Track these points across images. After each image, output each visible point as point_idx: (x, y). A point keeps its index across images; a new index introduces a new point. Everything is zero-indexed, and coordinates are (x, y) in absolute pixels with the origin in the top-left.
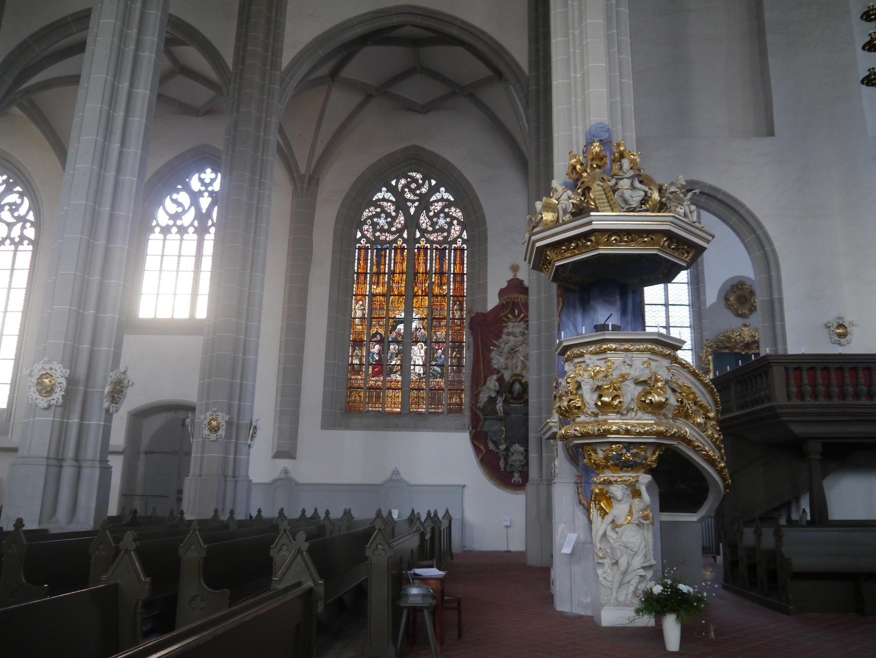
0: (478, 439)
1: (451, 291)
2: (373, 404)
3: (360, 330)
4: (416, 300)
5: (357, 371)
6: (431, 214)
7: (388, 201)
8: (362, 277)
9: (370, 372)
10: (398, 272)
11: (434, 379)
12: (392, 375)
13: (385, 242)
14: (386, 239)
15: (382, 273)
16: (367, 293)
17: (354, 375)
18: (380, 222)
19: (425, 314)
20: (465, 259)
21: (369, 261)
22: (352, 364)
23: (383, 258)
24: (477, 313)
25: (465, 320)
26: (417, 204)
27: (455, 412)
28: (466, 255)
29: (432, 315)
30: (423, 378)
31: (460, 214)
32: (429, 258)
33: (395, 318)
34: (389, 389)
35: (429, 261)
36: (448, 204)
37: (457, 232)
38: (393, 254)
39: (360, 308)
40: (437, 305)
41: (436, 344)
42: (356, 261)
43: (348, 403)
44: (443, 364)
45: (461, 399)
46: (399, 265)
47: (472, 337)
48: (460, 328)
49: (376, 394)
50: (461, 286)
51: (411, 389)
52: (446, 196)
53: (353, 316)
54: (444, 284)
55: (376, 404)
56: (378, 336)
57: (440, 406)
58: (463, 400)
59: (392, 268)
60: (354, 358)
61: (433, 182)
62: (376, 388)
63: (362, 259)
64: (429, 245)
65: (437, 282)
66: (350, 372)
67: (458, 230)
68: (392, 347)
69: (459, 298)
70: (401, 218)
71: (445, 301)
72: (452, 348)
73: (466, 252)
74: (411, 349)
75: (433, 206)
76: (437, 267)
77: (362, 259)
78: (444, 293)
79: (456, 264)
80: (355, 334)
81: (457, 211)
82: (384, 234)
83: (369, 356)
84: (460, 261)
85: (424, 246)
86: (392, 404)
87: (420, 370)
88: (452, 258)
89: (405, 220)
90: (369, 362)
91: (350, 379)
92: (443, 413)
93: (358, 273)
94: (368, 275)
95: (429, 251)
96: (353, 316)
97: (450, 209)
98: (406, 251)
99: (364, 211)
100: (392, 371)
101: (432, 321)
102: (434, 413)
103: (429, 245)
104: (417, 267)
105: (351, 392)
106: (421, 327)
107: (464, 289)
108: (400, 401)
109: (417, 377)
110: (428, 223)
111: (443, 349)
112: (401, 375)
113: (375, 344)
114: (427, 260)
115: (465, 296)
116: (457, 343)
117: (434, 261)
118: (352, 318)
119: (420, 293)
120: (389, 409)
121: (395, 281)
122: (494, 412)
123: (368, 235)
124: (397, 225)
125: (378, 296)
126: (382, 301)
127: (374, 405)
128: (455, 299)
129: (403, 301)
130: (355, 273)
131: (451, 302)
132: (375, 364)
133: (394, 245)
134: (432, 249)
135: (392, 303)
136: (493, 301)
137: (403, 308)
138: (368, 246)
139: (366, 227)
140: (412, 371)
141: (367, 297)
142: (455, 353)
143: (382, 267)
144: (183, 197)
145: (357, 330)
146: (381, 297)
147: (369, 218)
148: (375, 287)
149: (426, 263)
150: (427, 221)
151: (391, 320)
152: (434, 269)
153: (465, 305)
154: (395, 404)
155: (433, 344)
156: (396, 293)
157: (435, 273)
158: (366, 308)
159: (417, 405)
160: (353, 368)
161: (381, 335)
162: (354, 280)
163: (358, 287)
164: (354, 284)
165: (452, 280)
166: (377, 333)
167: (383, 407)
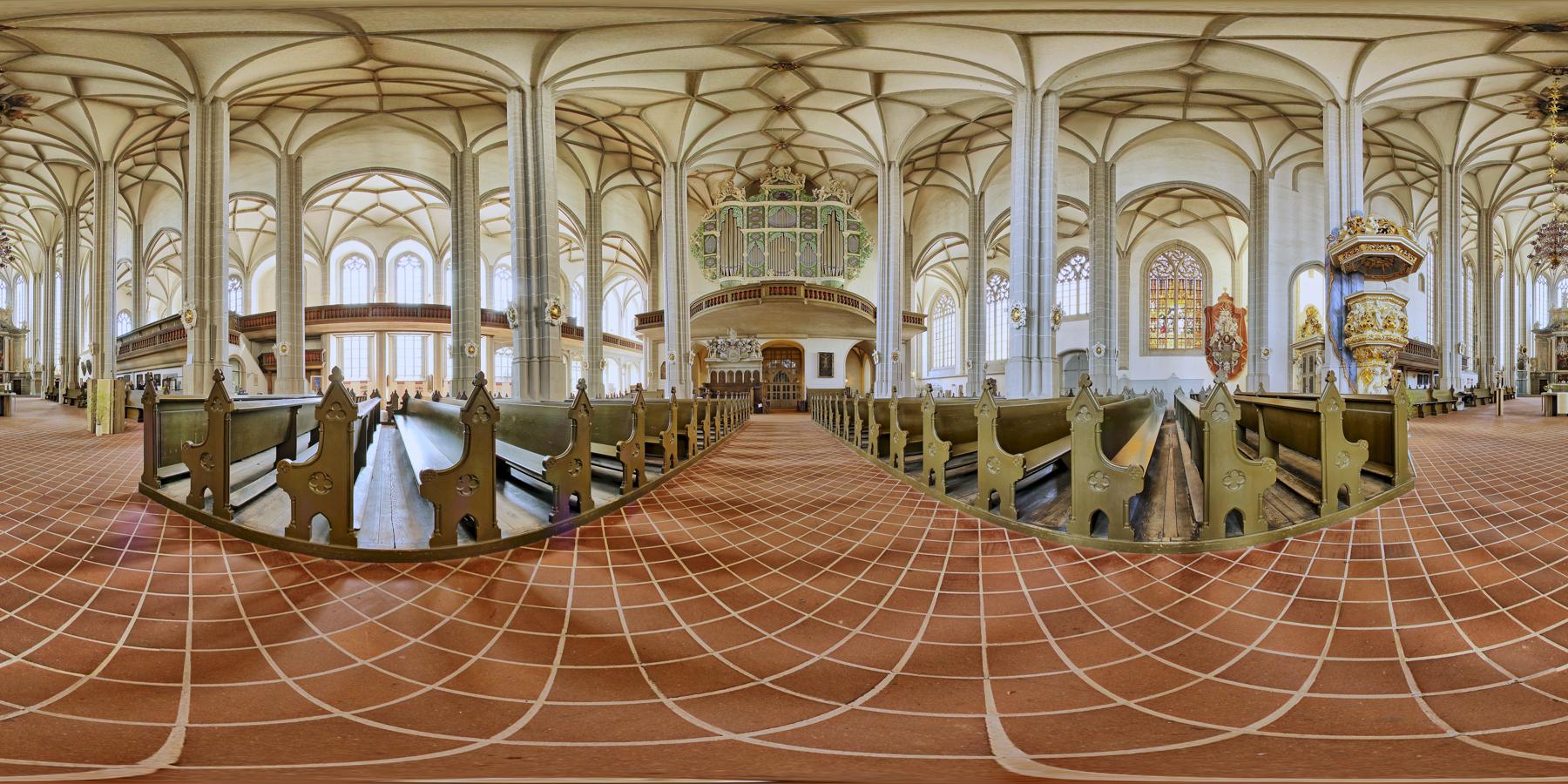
0: (1210, 358)
36: (1193, 262)
70: (1171, 268)
101: (1186, 309)
122: (1217, 348)
136: (1215, 302)
144: (1069, 268)
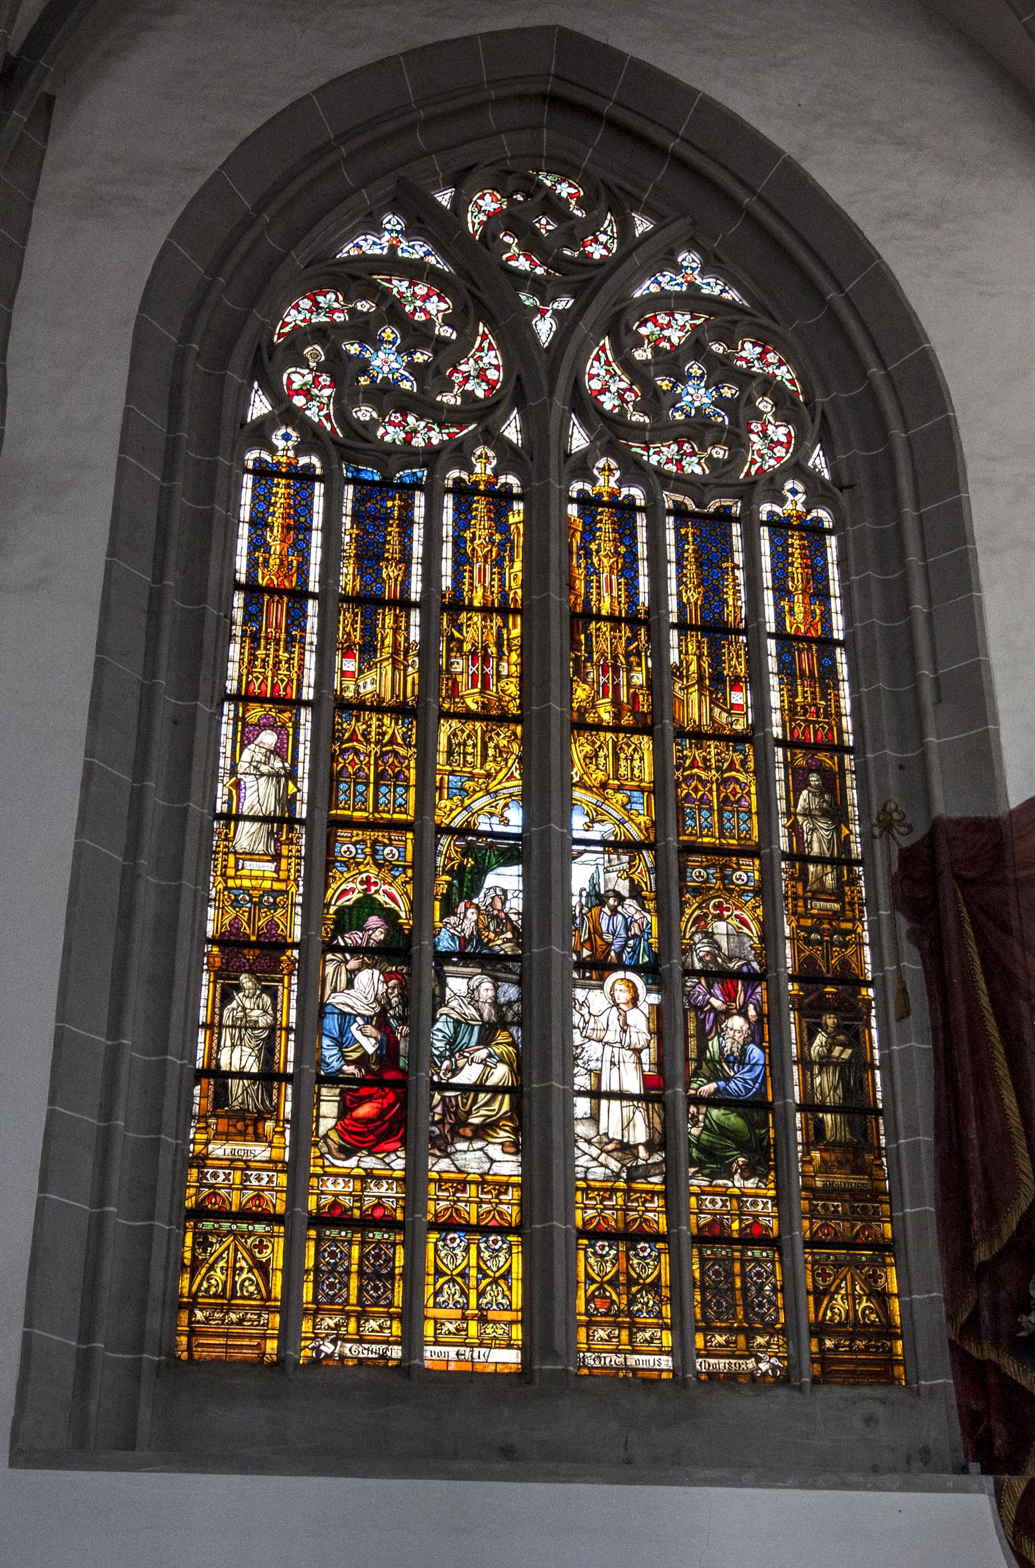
1: (776, 717)
2: (348, 1315)
3: (267, 884)
4: (588, 748)
5: (241, 1114)
6: (643, 354)
7: (415, 271)
8: (277, 612)
9: (326, 1125)
10: (476, 603)
11: (713, 1176)
12: (462, 1146)
13: (407, 454)
14: (407, 441)
15: (393, 603)
16: (308, 694)
17: (227, 1136)
18: (377, 363)
19: (642, 819)
20: (833, 572)
21: (316, 538)
22: (218, 1076)
23: (394, 529)
24: (936, 826)
25: (859, 870)
26: (564, 303)
27: (853, 1378)
28: (832, 554)
29: (681, 830)
30: (646, 1172)
31: (784, 373)
32: (642, 550)
33: (466, 831)
34: (445, 1226)
35: (643, 568)
37: (780, 451)
38: (448, 516)
39: (264, 769)
40: (704, 783)
41: (710, 987)
42: (244, 530)
43: (182, 1306)
44: (762, 1093)
45: (882, 1297)
46: (482, 571)
47: (916, 952)
48: (836, 906)
49: (363, 1257)
50: (824, 696)
51: (582, 1233)
52: (712, 287)
53: (220, 807)
54: (736, 684)
55: (362, 1316)
56: (373, 921)
57: (760, 1340)
58: (895, 1305)
59: (447, 582)
60: (226, 1034)
61: (642, 225)
62: (366, 1223)
63: (277, 521)
64: (637, 493)
65: (693, 667)
66: (203, 1117)
67: (784, 439)
68: (456, 985)
69: (821, 756)
71: (744, 763)
72: (801, 1009)
73: (832, 541)
74: (569, 1004)
75: (650, 325)
76: (693, 596)
77: (277, 521)
78: (739, 727)
79: (790, 594)
80: (236, 903)
81: (771, 357)
82: (396, 417)
83: (321, 1033)
84: (806, 581)
85: (613, 494)
86: (465, 1318)
87: (626, 1125)
88: (766, 562)
89: (508, 367)
90: (321, 1062)
91: (201, 1161)
92: (785, 1379)
93: (252, 589)
94: (312, 607)
95: (641, 520)
96: (220, 807)
97: (731, 344)
98: (518, 506)
99: (289, 300)
100: (466, 1124)
102: (732, 1377)
103: (637, 493)
104: (580, 585)
105: (202, 1241)
106: (623, 888)
107: (839, 715)
108: (517, 1300)
109: (615, 1165)
110: (629, 396)
111: (752, 1012)
112: (517, 1148)
113: (353, 964)
114: (632, 557)
115: (850, 750)
116: (830, 982)
117: (672, 570)
118: (219, 817)
119: (606, 717)
120: (452, 1352)
121: (467, 647)
123: (313, 414)
124: (469, 387)
125: (372, 709)
126: (393, 741)
127: (352, 1326)
128: (801, 762)
129: (515, 748)
130: (238, 586)
131: (780, 774)
132: (351, 1080)
133: (454, 474)
134: (653, 510)
135: (450, 753)
137: (515, 785)
138: (310, 466)
139: (299, 378)
140: (582, 1129)
141: (306, 715)
142: (820, 1039)
143: (390, 572)
145: (246, 883)
146: (387, 720)
147: (319, 333)
148: (351, 665)
149: (628, 570)
150: (623, 385)
151: (445, 840)
152: (673, 604)
153: (853, 795)
154: (483, 1320)
155: (699, 988)
156: (474, 707)
157: (682, 627)
158: (304, 768)
159: (619, 1326)
160: (221, 1097)
161: (390, 916)
162: (233, 623)
163: (253, 657)
164: (231, 637)
165: (772, 664)
166: (368, 905)
167: (411, 1341)
